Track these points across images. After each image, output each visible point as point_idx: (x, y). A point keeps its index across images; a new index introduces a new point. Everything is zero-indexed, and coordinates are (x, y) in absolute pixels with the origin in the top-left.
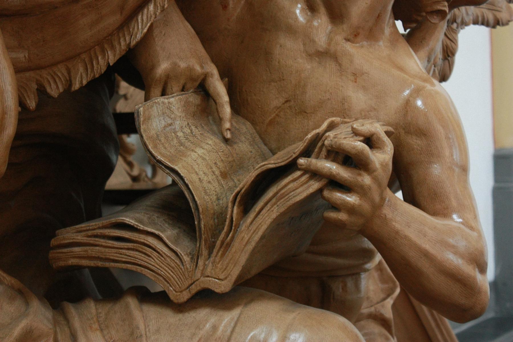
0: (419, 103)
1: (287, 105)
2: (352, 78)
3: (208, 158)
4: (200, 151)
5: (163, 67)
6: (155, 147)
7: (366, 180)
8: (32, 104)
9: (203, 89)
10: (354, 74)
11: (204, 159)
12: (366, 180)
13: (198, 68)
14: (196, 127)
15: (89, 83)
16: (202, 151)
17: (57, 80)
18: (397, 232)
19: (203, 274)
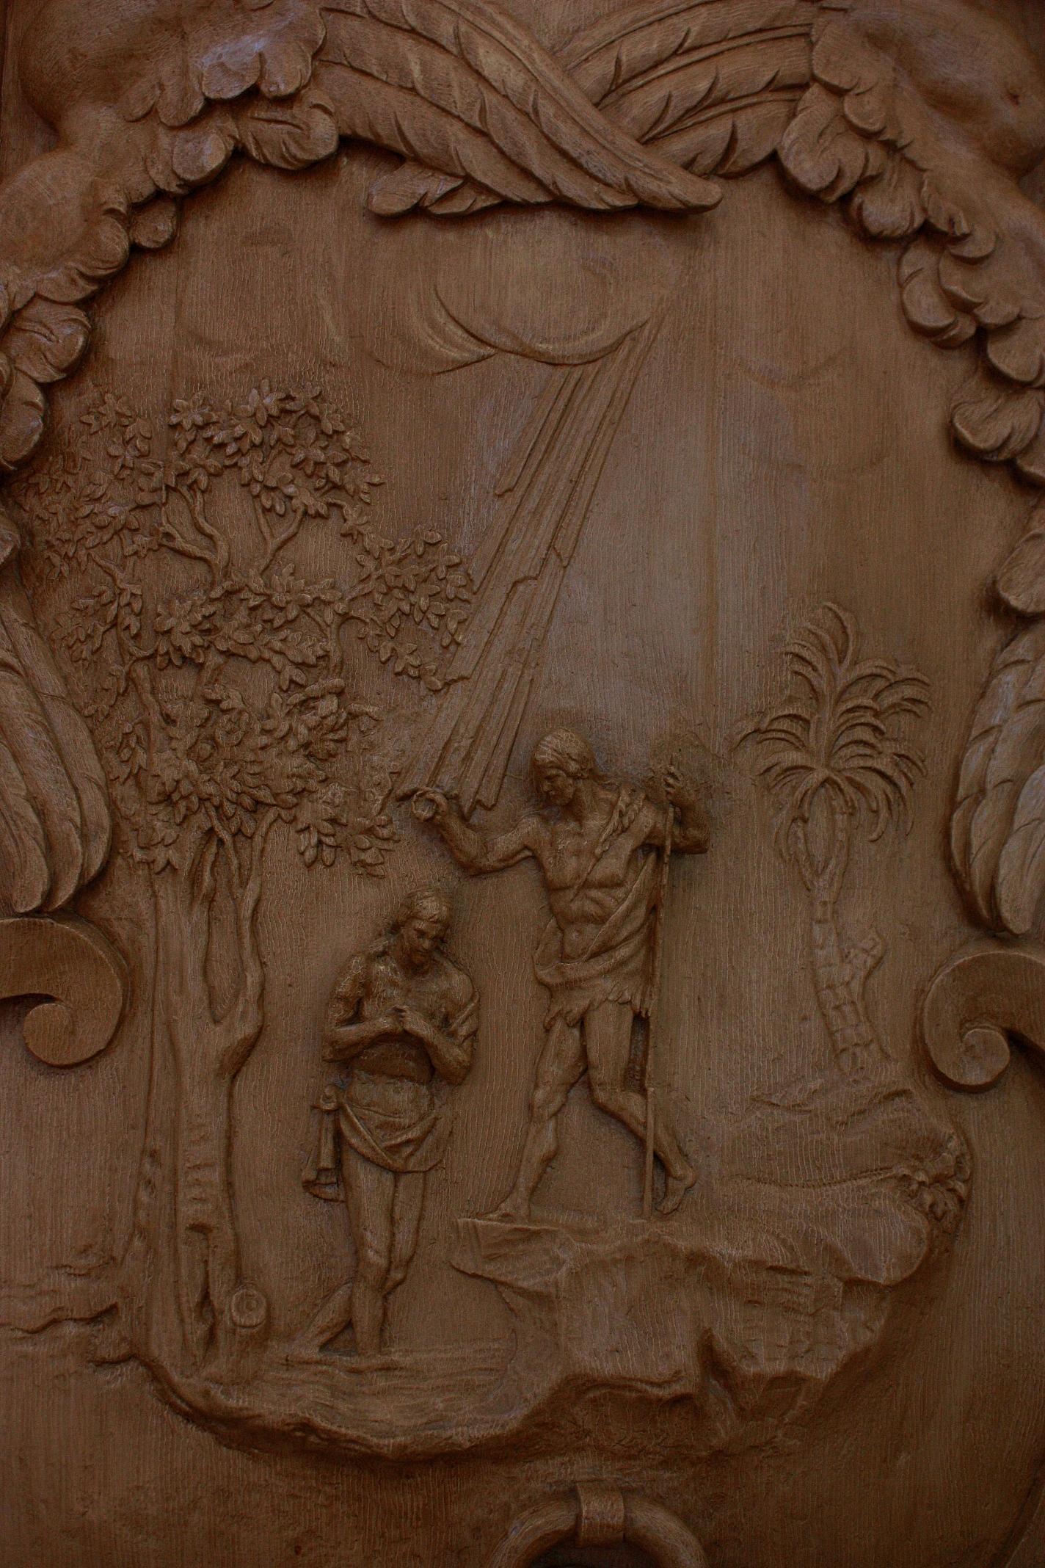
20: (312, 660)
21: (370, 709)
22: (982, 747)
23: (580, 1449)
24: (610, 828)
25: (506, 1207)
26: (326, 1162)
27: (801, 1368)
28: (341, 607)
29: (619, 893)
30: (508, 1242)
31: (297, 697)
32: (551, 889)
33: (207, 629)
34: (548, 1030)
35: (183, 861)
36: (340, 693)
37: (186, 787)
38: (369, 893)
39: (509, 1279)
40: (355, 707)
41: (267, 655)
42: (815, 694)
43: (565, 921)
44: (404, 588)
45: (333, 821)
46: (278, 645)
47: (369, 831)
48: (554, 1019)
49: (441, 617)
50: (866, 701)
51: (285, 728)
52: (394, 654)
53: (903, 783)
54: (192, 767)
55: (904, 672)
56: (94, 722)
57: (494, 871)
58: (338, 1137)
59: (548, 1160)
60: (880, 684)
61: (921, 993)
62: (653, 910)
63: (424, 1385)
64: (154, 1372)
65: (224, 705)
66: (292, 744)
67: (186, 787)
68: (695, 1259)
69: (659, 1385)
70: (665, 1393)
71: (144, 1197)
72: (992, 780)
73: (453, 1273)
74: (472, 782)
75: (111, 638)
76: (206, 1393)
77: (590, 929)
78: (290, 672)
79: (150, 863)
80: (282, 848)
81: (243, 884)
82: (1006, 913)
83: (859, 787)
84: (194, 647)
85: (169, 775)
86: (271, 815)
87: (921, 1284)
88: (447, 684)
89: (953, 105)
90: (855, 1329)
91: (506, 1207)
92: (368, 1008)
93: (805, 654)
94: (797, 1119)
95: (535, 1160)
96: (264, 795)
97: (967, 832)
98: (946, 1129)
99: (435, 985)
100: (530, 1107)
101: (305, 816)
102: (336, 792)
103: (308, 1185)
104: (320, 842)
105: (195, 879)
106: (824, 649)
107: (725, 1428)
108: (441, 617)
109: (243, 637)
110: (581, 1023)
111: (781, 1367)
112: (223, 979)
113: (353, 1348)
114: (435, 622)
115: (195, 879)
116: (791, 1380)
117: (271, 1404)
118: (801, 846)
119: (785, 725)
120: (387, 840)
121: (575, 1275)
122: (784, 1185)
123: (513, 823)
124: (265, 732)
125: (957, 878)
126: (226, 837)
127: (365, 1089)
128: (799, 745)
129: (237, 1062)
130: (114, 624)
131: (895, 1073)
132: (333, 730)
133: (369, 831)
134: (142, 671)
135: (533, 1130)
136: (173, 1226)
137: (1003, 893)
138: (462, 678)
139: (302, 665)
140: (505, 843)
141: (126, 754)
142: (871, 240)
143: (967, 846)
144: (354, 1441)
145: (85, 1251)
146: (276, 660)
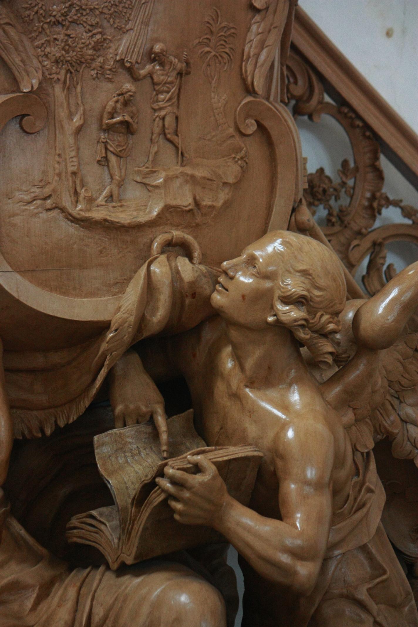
0: (290, 434)
1: (222, 431)
2: (248, 414)
3: (140, 472)
4: (137, 467)
5: (119, 408)
6: (104, 464)
7: (187, 494)
8: (48, 432)
9: (151, 421)
10: (250, 412)
11: (137, 473)
12: (187, 494)
13: (144, 409)
14: (145, 449)
15: (78, 419)
16: (141, 467)
17: (64, 416)
18: (229, 529)
19: (121, 551)
20: (94, 24)
21: (109, 37)
22: (249, 45)
23: (166, 224)
24: (172, 68)
25: (146, 165)
26: (104, 155)
27: (214, 204)
28: (100, 10)
29: (173, 85)
30: (148, 174)
31: (90, 34)
32: (154, 84)
33: (65, 15)
34: (154, 120)
35: (62, 77)
36: (100, 33)
37: (62, 58)
38: (110, 85)
39: (149, 183)
40: (105, 37)
41: (82, 22)
42: (212, 33)
43: (159, 92)
44: (116, 5)
45: (101, 67)
46: (85, 20)
47: (110, 70)
48: (156, 118)
49: (125, 13)
50: (223, 33)
51: (88, 42)
52: (114, 23)
53: (231, 55)
54: (64, 52)
55: (231, 25)
56: (32, 40)
57: (142, 79)
58: (106, 149)
59: (156, 153)
60: (226, 29)
61: (236, 110)
62: (179, 89)
63: (131, 209)
64: (63, 210)
65: (72, 36)
66: (90, 46)
67: (62, 58)
68: (192, 177)
69: (186, 207)
70: (187, 209)
71: (57, 165)
72: (252, 54)
73: (135, 183)
74: (135, 57)
75: (36, 17)
76: (79, 214)
77: (165, 94)
78: (88, 27)
79: (51, 79)
81: (77, 84)
82: (256, 89)
83: (222, 57)
84: (62, 20)
85: (58, 55)
86: (84, 65)
87: (236, 186)
88: (127, 31)
90: (223, 196)
91: (146, 165)
92: (115, 115)
93: (210, 22)
94: (210, 142)
95: (153, 153)
96: (83, 60)
97: (246, 67)
98: (243, 145)
99: (129, 109)
100: (151, 140)
101: (94, 65)
102: (101, 59)
103: (98, 162)
104: (97, 73)
105: (65, 82)
106: (213, 20)
107: (199, 219)
108: (125, 13)
109: (75, 17)
110: (163, 119)
111: (210, 203)
112: (73, 109)
113: (112, 201)
114: (124, 14)
115: (65, 82)
116: (212, 207)
117: (97, 215)
118: (209, 72)
119: (205, 41)
120: (114, 72)
121: (165, 180)
122: (208, 159)
123: (144, 66)
124: (82, 43)
126: (73, 71)
128: (208, 46)
129: (79, 131)
130: (37, 12)
131: (231, 130)
132: (100, 43)
133: (110, 70)
134: (46, 26)
135: (152, 146)
136: (66, 173)
137: (255, 83)
138: (131, 29)
139: (92, 26)
140: (142, 72)
141: (43, 49)
143: (246, 72)
144: (117, 223)
145: (41, 180)
146: (85, 25)
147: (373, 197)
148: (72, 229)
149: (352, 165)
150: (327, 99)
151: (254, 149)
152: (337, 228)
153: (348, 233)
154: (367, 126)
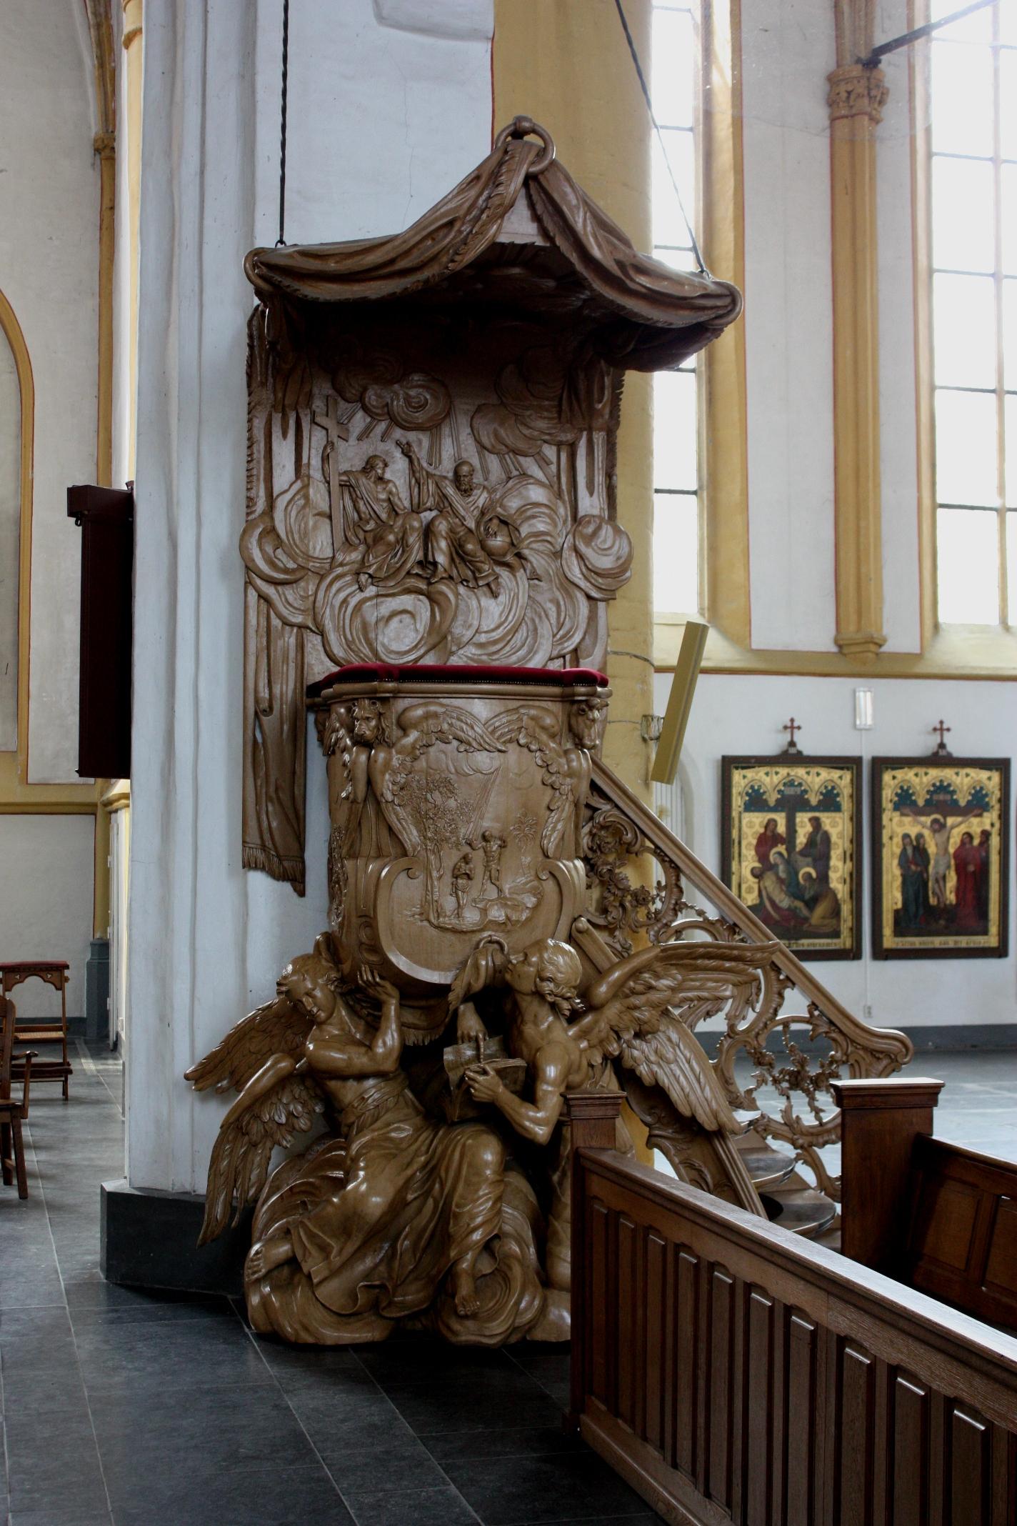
80: (446, 846)
87: (536, 908)
89: (544, 728)
116: (518, 921)
125: (543, 850)
127: (460, 881)
129: (440, 877)
142: (530, 751)
147: (676, 904)
148: (434, 932)
149: (663, 883)
150: (648, 844)
151: (550, 886)
152: (652, 921)
153: (659, 925)
154: (671, 861)
